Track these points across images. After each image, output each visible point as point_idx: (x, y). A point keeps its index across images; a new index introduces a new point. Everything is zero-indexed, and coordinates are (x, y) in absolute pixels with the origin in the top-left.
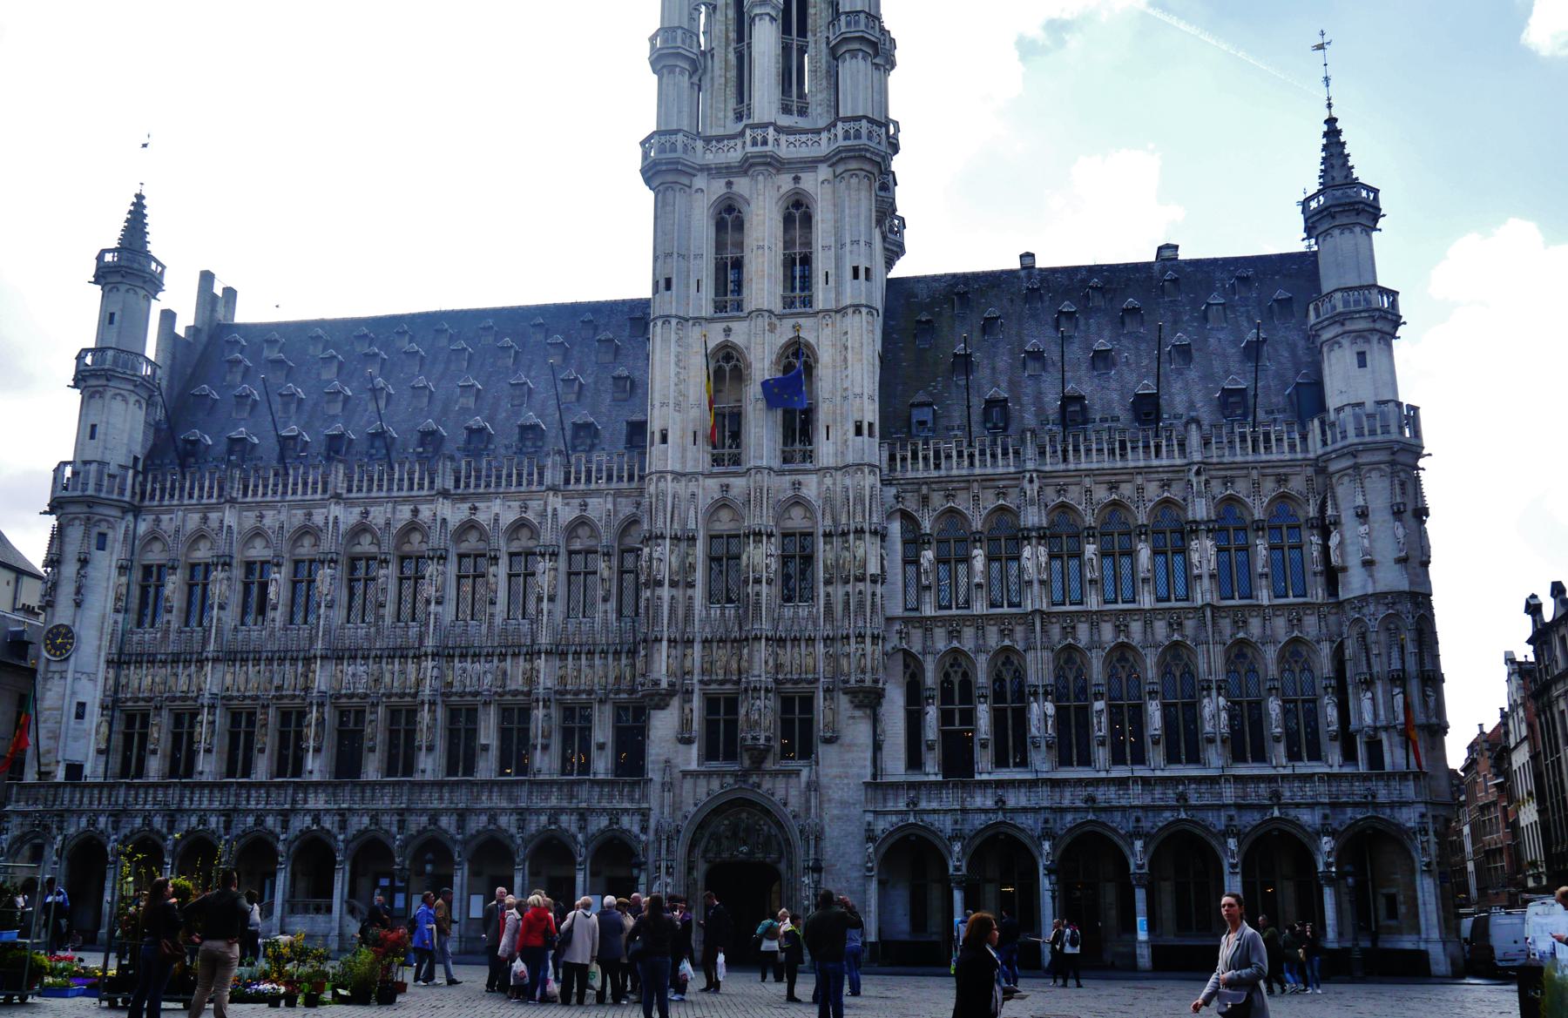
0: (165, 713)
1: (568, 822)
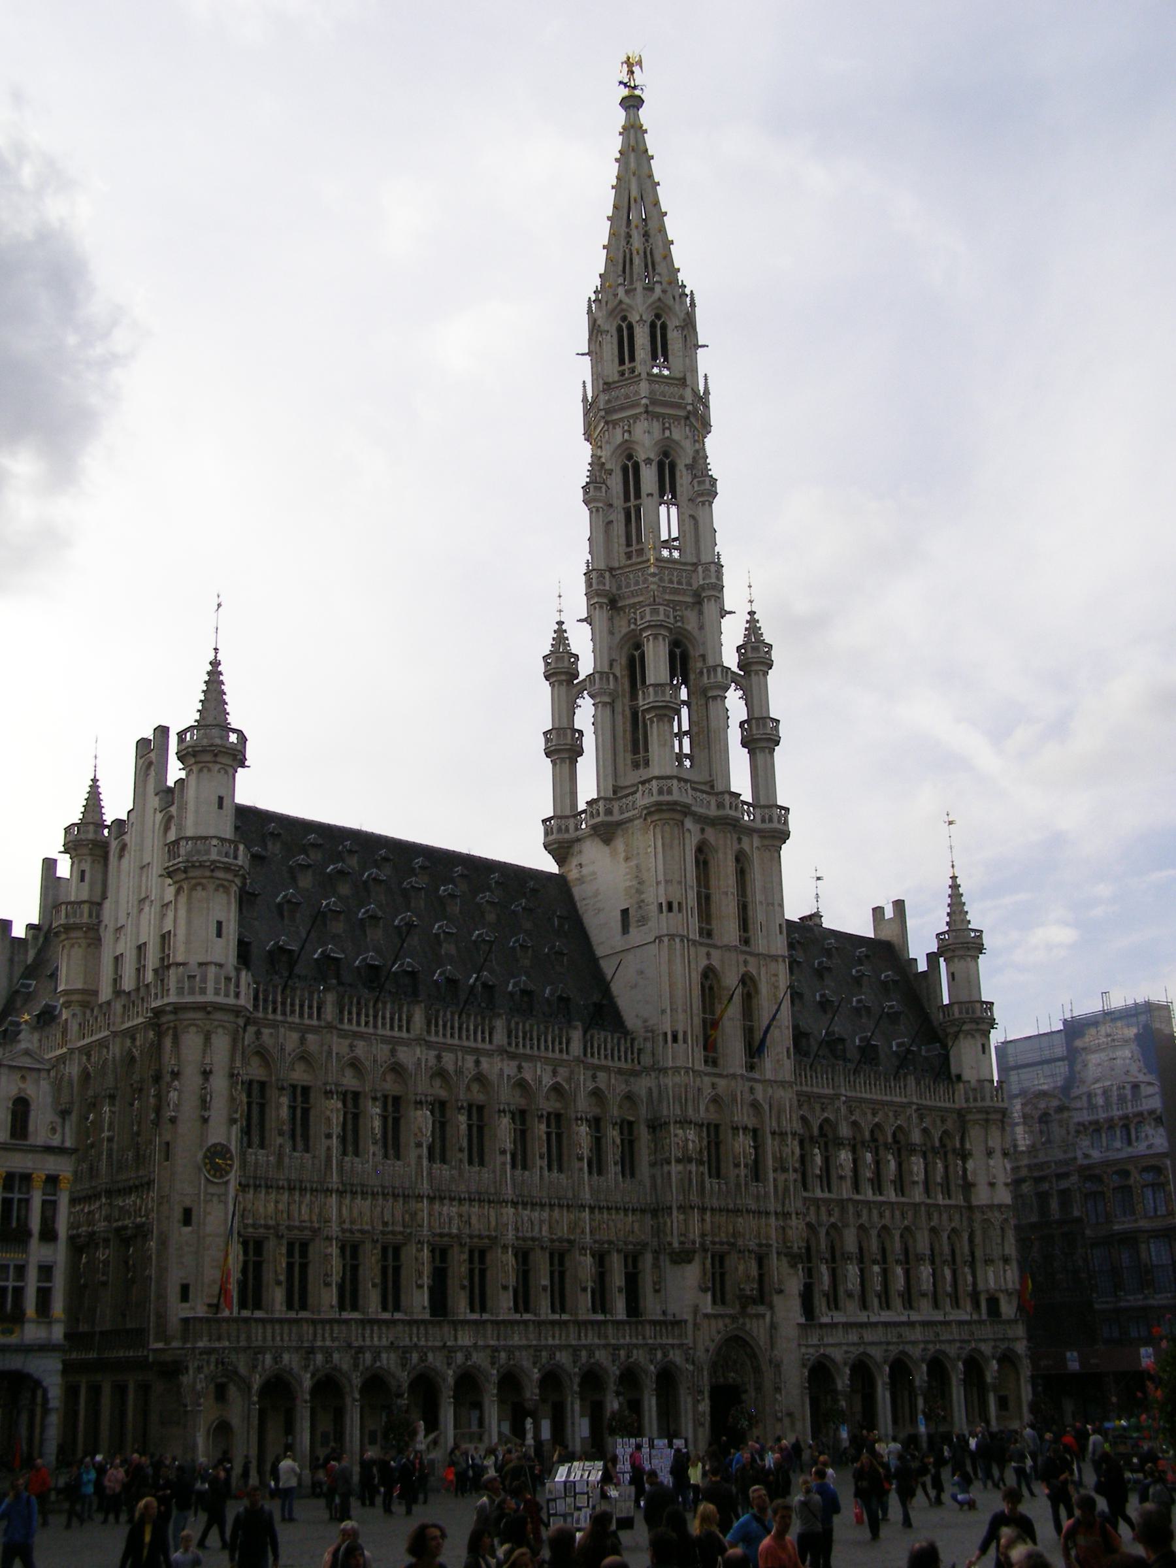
0: (285, 1242)
1: (639, 1356)
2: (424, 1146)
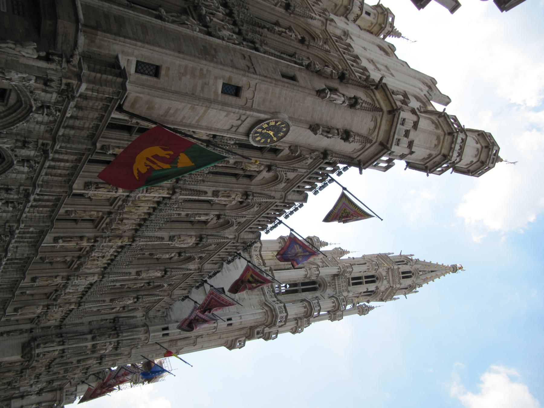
2: (170, 243)
